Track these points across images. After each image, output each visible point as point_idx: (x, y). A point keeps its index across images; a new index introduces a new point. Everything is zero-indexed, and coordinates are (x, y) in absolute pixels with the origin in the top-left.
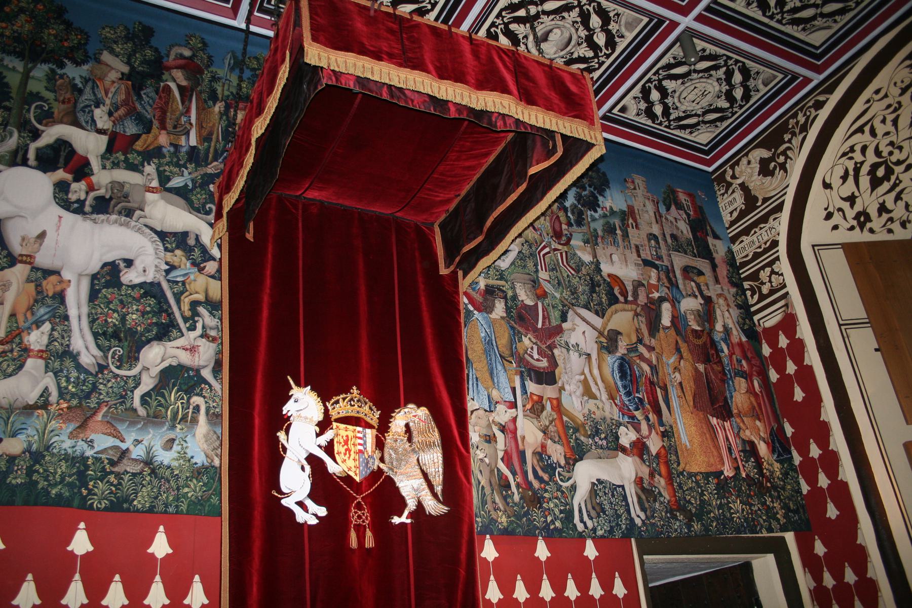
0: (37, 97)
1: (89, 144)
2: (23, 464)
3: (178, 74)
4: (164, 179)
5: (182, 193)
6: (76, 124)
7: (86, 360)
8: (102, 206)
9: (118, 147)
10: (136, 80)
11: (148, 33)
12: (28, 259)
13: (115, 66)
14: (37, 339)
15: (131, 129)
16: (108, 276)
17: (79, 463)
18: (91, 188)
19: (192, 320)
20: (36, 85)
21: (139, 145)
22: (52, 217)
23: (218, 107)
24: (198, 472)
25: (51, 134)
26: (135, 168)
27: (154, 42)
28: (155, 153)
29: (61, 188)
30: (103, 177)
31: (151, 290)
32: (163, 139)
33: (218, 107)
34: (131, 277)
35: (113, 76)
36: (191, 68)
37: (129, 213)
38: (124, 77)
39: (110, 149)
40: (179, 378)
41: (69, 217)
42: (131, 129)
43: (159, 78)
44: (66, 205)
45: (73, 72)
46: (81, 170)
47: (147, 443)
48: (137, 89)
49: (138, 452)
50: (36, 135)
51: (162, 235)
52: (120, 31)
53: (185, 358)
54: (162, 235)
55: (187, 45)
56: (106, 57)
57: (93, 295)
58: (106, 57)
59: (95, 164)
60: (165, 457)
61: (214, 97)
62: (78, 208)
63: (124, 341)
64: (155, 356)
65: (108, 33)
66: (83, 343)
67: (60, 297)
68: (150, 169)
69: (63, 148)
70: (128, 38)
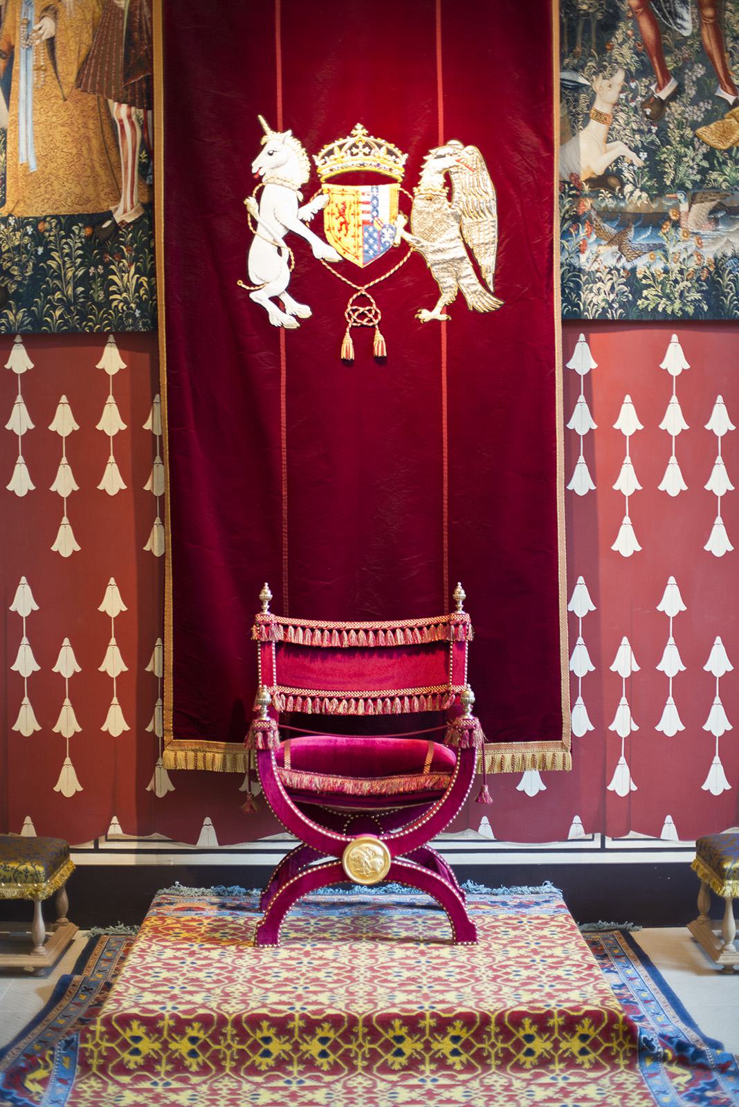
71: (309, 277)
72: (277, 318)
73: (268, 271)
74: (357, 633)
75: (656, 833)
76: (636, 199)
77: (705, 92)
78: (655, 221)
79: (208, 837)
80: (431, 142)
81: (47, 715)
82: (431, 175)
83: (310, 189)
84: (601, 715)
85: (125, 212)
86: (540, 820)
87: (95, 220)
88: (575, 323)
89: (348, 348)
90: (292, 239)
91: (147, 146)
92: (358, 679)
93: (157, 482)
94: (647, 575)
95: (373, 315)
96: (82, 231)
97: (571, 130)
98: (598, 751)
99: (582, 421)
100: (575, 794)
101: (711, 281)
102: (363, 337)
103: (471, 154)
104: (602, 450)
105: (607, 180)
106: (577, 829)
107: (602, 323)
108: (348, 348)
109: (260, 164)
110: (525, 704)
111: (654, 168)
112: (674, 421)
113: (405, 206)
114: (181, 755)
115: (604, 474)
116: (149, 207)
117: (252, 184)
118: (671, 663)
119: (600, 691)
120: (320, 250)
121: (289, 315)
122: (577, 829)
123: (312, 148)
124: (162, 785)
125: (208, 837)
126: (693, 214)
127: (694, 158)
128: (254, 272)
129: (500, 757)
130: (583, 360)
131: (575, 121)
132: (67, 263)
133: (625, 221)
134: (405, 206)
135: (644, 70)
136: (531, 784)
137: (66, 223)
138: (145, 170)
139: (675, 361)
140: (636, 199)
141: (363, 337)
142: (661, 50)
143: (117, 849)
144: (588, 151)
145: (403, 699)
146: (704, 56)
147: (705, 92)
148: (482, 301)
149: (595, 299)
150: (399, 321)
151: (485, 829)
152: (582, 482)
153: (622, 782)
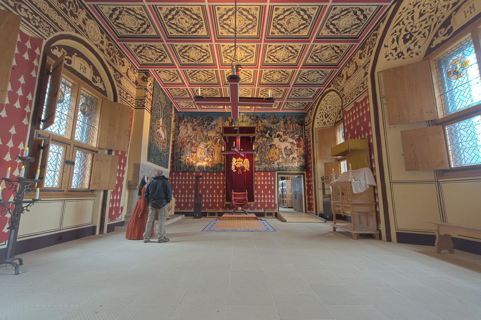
0: (275, 129)
1: (281, 133)
2: (281, 168)
3: (289, 121)
4: (289, 136)
5: (291, 137)
6: (280, 131)
7: (285, 157)
8: (284, 141)
9: (284, 133)
10: (285, 123)
11: (285, 116)
12: (278, 148)
13: (282, 122)
14: (280, 156)
15: (285, 130)
16: (286, 148)
17: (286, 167)
18: (282, 139)
19: (294, 152)
20: (275, 128)
21: (286, 132)
22: (279, 143)
23: (294, 125)
24: (296, 167)
25: (277, 133)
26: (286, 135)
27: (286, 117)
28: (288, 133)
29: (280, 139)
30: (283, 137)
31: (290, 149)
32: (289, 131)
33: (294, 125)
34: (288, 148)
35: (282, 124)
36: (290, 120)
37: (286, 141)
38: (283, 123)
39: (283, 134)
40: (293, 158)
41: (281, 143)
42: (285, 130)
43: (287, 122)
44: (280, 141)
45: (278, 124)
46: (281, 137)
47: (291, 165)
48: (285, 125)
49: (291, 166)
50: (276, 134)
51: (290, 143)
52: (282, 117)
53: (294, 156)
54: (290, 143)
55: (289, 116)
56: (281, 121)
57: (285, 151)
58: (281, 121)
59: (282, 136)
60: (293, 166)
61: (293, 123)
62: (281, 141)
63: (288, 155)
64: (291, 156)
65: (280, 118)
66: (284, 156)
67: (282, 151)
68: (288, 135)
69: (279, 134)
70: (283, 118)
71: (236, 168)
72: (234, 171)
73: (233, 168)
74: (239, 193)
75: (262, 209)
76: (260, 163)
77: (264, 155)
78: (261, 164)
79: (228, 210)
80: (245, 159)
81: (216, 200)
82: (245, 161)
83: (236, 162)
84: (257, 200)
85: (223, 163)
86: (252, 209)
87: (221, 164)
88: (255, 171)
89: (239, 173)
90: (235, 165)
91: (224, 159)
92: (239, 197)
93: (225, 183)
94: (261, 190)
95: (241, 171)
96: (220, 165)
97: (255, 158)
98: (257, 203)
99: (256, 179)
100: (256, 206)
101: (265, 169)
102: (240, 172)
103: (247, 159)
104: (257, 181)
105: (257, 161)
106: (256, 209)
107: (257, 171)
108: (239, 173)
109: (233, 160)
110: (251, 199)
111: (261, 160)
112: (262, 179)
113: (243, 163)
114: (226, 203)
115: (257, 182)
116: (225, 163)
117: (232, 162)
118: (263, 196)
119: (257, 198)
120: (237, 166)
121: (235, 171)
122: (256, 209)
123: (236, 159)
124: (224, 205)
125: (228, 210)
126: (264, 164)
127: (264, 160)
128: (232, 168)
129: (250, 203)
130: (256, 174)
131: (255, 157)
132: (218, 167)
133: (258, 164)
134: (243, 163)
135: (260, 153)
136: (252, 206)
137: (219, 164)
138: (224, 160)
139: (262, 174)
140: (260, 163)
141: (240, 172)
142: (261, 152)
143: (221, 210)
144: (256, 159)
145: (243, 198)
146: (264, 152)
147: (264, 155)
148: (248, 170)
149: (257, 170)
150: (242, 171)
151: (249, 209)
152: (256, 183)
153: (259, 206)
